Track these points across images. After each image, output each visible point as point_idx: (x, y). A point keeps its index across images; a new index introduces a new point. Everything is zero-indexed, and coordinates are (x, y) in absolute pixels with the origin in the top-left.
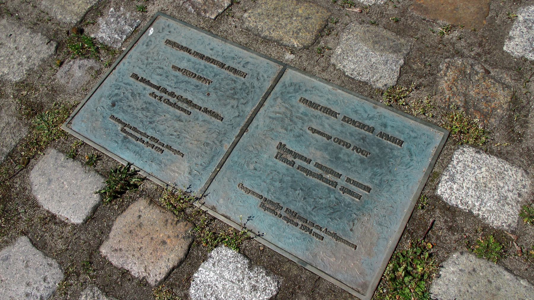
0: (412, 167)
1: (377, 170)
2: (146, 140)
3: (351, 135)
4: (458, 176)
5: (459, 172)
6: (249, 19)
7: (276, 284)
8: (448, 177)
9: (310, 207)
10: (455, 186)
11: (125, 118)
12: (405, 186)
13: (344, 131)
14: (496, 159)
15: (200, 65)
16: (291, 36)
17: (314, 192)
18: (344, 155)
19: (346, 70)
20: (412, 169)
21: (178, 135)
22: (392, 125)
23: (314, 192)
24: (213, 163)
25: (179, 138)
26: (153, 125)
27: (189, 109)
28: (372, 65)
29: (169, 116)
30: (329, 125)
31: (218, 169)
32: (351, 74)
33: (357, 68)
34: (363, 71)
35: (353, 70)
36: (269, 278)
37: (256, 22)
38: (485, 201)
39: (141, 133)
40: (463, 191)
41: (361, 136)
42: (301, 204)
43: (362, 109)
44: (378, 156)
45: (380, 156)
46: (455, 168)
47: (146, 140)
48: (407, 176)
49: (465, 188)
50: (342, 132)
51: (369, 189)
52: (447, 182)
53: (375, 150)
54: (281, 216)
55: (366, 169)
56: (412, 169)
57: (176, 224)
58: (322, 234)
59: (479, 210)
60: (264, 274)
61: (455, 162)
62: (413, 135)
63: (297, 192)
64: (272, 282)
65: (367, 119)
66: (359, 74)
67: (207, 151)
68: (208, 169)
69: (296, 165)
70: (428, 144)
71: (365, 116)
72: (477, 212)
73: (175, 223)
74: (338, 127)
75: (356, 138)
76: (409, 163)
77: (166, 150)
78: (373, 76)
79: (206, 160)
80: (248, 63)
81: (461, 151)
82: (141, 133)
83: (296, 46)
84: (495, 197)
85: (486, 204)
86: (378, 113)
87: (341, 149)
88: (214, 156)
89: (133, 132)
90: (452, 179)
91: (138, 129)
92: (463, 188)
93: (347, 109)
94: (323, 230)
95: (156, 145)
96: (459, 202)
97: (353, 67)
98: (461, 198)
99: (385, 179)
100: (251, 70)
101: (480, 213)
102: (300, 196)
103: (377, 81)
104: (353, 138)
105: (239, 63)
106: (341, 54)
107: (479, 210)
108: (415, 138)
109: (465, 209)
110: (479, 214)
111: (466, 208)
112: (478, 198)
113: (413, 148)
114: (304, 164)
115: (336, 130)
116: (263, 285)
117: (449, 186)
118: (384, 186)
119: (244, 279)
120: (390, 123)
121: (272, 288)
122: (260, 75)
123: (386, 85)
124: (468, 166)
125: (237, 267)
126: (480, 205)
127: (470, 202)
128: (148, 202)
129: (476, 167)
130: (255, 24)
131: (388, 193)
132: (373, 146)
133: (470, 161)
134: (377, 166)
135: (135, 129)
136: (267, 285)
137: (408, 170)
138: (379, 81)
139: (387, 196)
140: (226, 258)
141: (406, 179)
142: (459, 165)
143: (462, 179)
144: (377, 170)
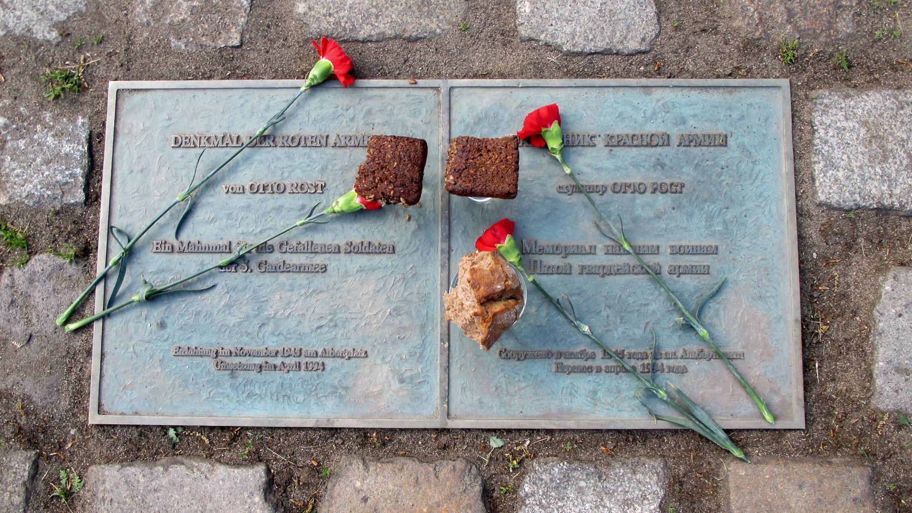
0: (761, 174)
1: (710, 208)
2: (278, 361)
3: (636, 165)
4: (837, 153)
5: (836, 147)
6: (313, 13)
7: (655, 478)
8: (822, 164)
9: (638, 327)
10: (840, 174)
11: (205, 339)
12: (766, 213)
13: (620, 163)
14: (878, 95)
15: (278, 159)
16: (417, 14)
17: (631, 300)
18: (643, 207)
19: (559, 41)
20: (763, 178)
21: (331, 320)
22: (692, 113)
23: (631, 300)
24: (429, 339)
25: (336, 326)
26: (269, 328)
27: (319, 259)
28: (600, 11)
29: (289, 294)
30: (589, 166)
31: (446, 345)
32: (574, 45)
33: (578, 29)
34: (591, 29)
35: (573, 35)
36: (639, 476)
37: (330, 15)
38: (894, 175)
39: (258, 354)
40: (855, 176)
41: (653, 159)
42: (620, 330)
43: (628, 108)
44: (699, 181)
45: (702, 180)
46: (826, 142)
47: (278, 361)
48: (760, 195)
49: (856, 170)
50: (617, 169)
51: (714, 251)
52: (825, 173)
53: (687, 175)
54: (599, 370)
55: (691, 215)
56: (763, 178)
57: (437, 477)
58: (682, 363)
59: (891, 196)
60: (629, 475)
61: (822, 132)
62: (735, 115)
63: (604, 313)
64: (648, 480)
65: (646, 122)
66: (586, 39)
67: (406, 323)
68: (427, 353)
69: (576, 270)
70: (766, 121)
71: (639, 117)
72: (890, 201)
73: (433, 476)
74: (609, 164)
75: (647, 165)
76: (752, 170)
77: (329, 362)
78: (614, 31)
79: (416, 340)
80: (369, 112)
81: (822, 107)
82: (258, 354)
83: (438, 31)
84: (905, 162)
85: (896, 181)
86: (658, 101)
87: (634, 200)
88: (423, 326)
89: (244, 360)
90: (831, 164)
91: (246, 348)
92: (853, 171)
93: (602, 118)
94: (679, 354)
95: (303, 360)
96: (858, 199)
97: (568, 29)
98: (858, 190)
99: (729, 216)
100: (384, 125)
101: (894, 199)
102: (612, 318)
103: (625, 38)
104: (642, 169)
105: (352, 120)
106: (532, 11)
107: (891, 196)
108: (742, 117)
109: (871, 205)
110: (893, 202)
111: (871, 202)
112: (882, 176)
113: (746, 140)
114: (588, 261)
115: (606, 169)
116: (637, 492)
117: (832, 180)
118: (735, 229)
119: (602, 500)
120: (687, 112)
121: (654, 489)
122: (409, 124)
123: (643, 39)
124: (844, 129)
125: (580, 488)
126: (889, 186)
127: (874, 191)
128: (361, 466)
129: (857, 125)
130: (332, 20)
131: (747, 239)
132: (682, 168)
133: (842, 118)
134: (705, 201)
135: (241, 353)
136: (643, 489)
137: (758, 182)
138: (629, 37)
139: (747, 244)
140: (554, 484)
141: (761, 200)
142: (831, 134)
143: (845, 157)
144: (710, 208)
